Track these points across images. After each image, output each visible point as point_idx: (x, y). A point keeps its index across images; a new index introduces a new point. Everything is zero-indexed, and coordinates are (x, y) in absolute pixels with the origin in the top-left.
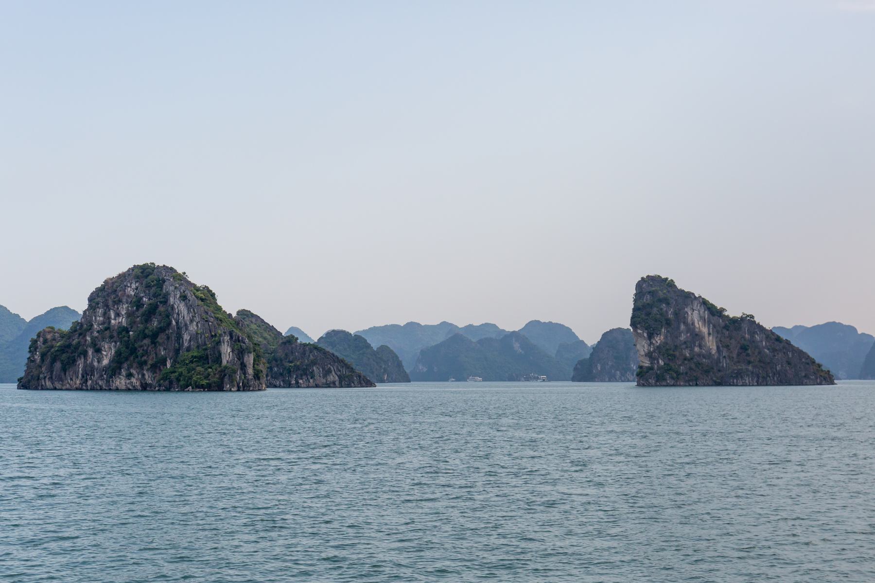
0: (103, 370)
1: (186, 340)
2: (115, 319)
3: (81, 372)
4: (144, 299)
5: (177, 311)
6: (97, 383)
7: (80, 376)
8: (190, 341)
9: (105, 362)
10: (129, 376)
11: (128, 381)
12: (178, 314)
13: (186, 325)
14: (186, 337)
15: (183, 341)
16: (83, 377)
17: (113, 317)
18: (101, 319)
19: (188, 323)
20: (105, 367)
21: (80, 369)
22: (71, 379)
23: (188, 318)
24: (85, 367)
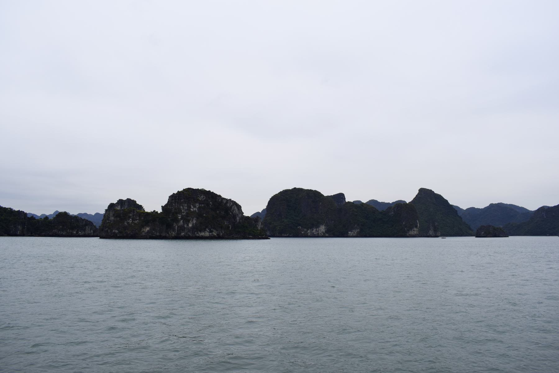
0: (191, 229)
1: (238, 220)
2: (193, 209)
3: (176, 229)
4: (210, 203)
5: (233, 209)
6: (187, 234)
7: (176, 231)
8: (240, 220)
9: (190, 225)
10: (211, 232)
11: (210, 233)
12: (233, 210)
13: (237, 214)
14: (238, 218)
15: (236, 220)
16: (177, 230)
17: (192, 208)
18: (186, 208)
19: (238, 214)
20: (191, 227)
21: (176, 228)
22: (170, 232)
23: (238, 212)
24: (178, 227)
